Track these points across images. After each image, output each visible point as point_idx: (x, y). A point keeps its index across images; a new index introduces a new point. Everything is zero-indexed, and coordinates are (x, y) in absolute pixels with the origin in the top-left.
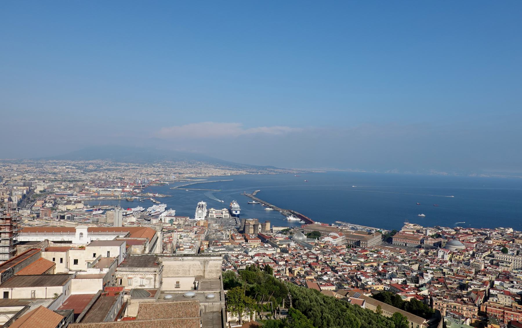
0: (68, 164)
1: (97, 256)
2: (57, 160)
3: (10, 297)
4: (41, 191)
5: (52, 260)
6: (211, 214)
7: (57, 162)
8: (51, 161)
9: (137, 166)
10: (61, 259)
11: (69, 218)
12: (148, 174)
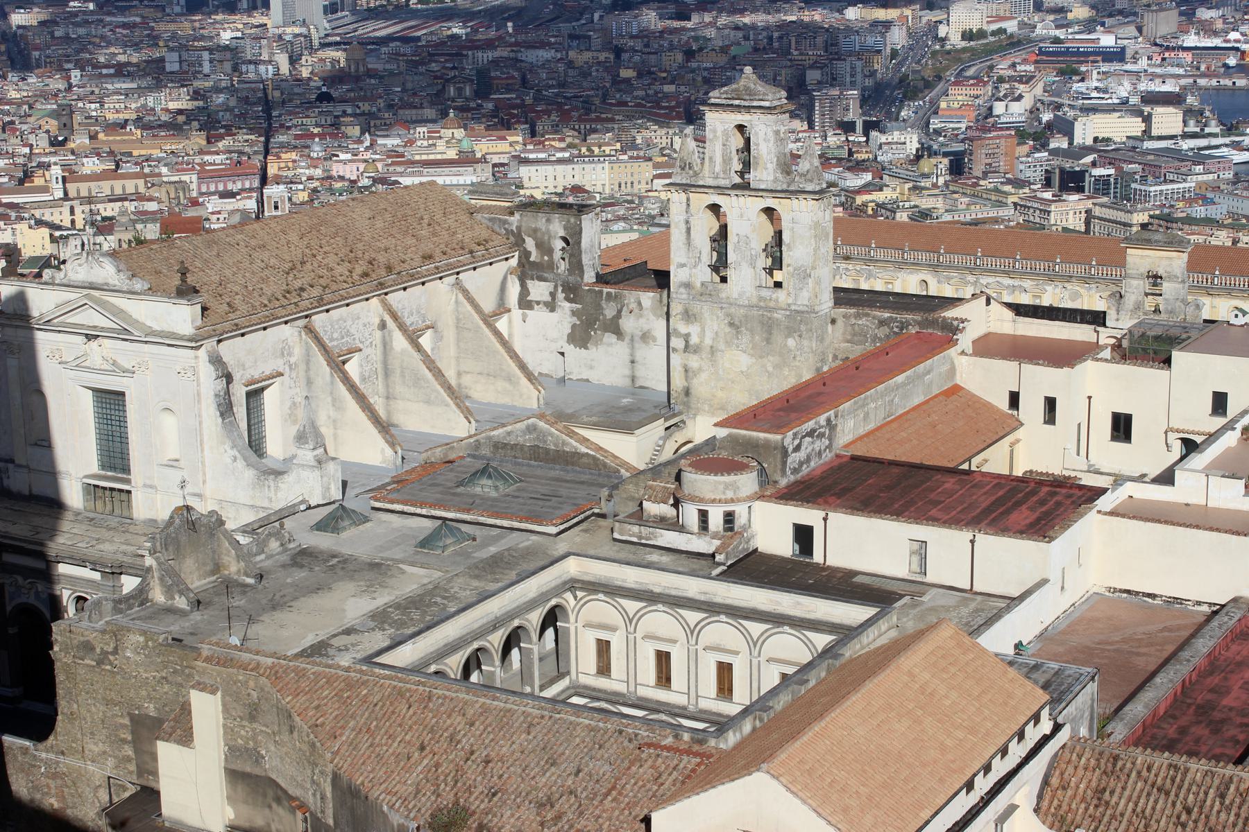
3: (818, 557)
4: (968, 35)
5: (1003, 404)
10: (1051, 404)
11: (1103, 186)
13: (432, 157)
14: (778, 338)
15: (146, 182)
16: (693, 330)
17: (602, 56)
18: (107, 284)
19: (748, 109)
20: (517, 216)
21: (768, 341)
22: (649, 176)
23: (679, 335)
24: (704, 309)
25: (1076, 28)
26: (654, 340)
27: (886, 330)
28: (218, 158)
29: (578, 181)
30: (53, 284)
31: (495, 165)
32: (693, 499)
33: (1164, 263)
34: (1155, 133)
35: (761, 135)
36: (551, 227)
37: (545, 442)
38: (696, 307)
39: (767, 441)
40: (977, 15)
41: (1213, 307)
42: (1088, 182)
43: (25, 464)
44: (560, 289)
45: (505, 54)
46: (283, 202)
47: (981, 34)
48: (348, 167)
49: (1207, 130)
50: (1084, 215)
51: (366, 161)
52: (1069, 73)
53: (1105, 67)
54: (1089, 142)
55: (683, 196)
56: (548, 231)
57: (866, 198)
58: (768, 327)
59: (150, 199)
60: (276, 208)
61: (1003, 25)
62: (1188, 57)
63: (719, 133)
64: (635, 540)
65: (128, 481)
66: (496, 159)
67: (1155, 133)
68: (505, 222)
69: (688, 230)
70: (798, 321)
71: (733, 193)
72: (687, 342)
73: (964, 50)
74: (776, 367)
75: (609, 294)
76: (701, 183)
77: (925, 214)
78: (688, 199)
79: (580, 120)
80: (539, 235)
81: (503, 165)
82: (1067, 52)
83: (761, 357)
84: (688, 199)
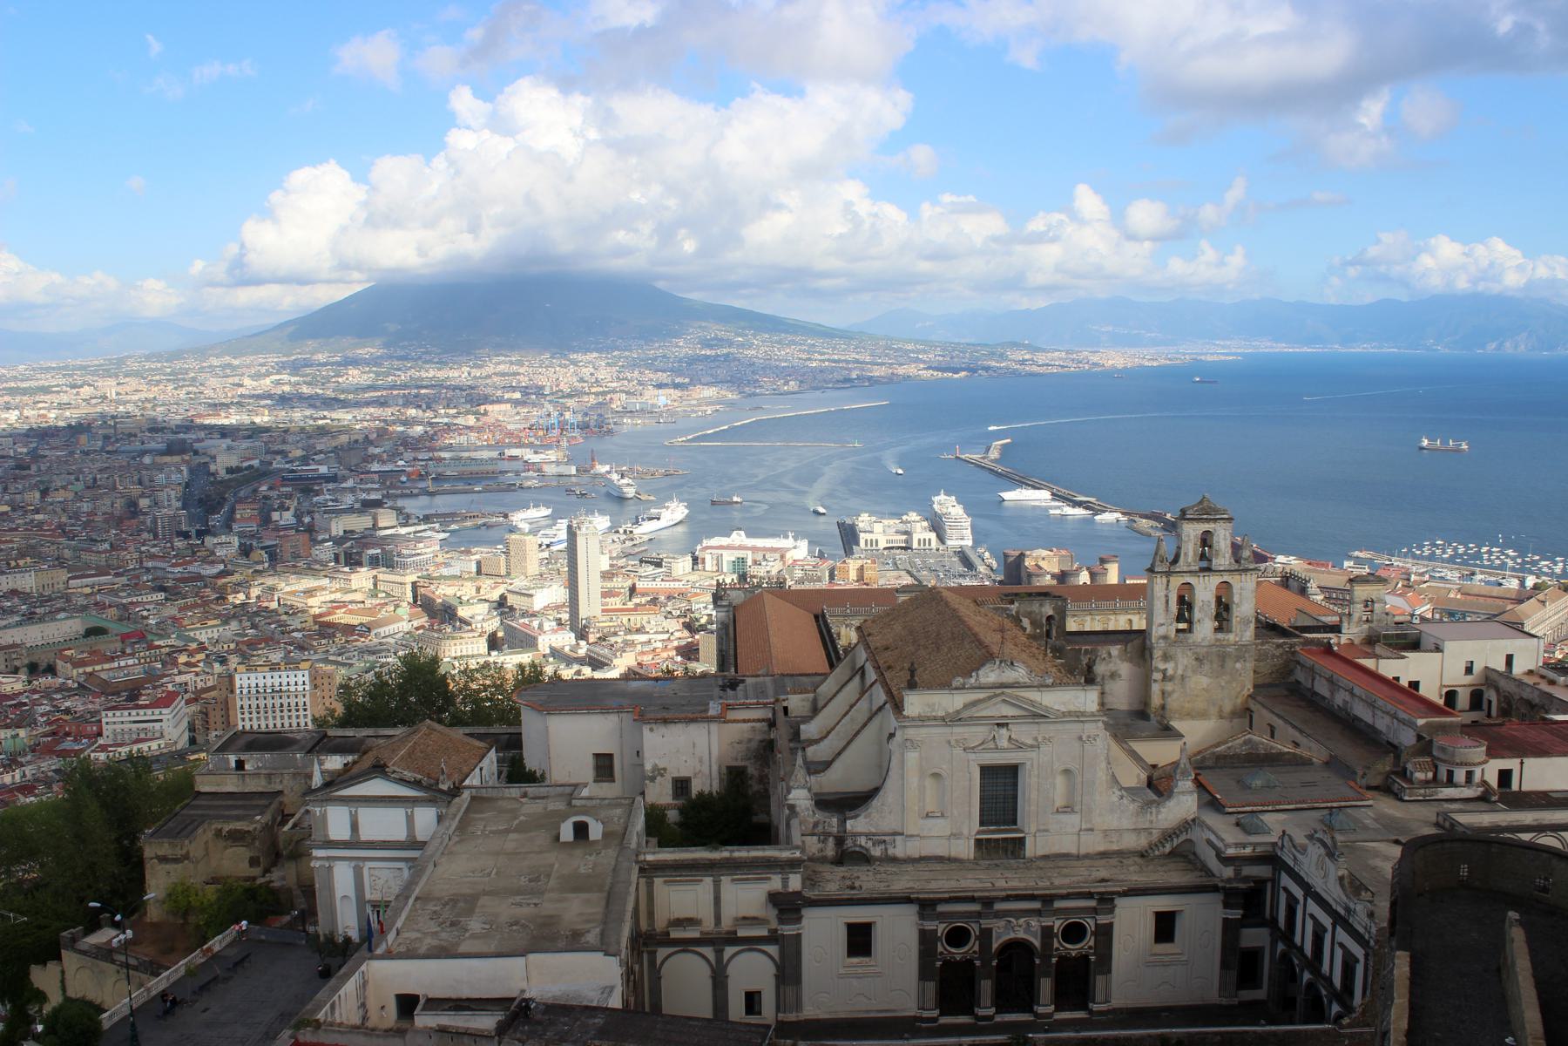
0: (273, 367)
1: (1477, 668)
2: (235, 358)
3: (1515, 787)
4: (230, 470)
6: (869, 536)
7: (236, 362)
8: (215, 362)
9: (512, 363)
12: (562, 391)
14: (1229, 664)
16: (1170, 667)
18: (1018, 683)
19: (1215, 520)
20: (1016, 604)
21: (1223, 666)
23: (1157, 670)
25: (297, 463)
26: (1120, 676)
29: (11, 586)
30: (963, 688)
32: (1461, 764)
33: (1375, 592)
34: (380, 525)
35: (1222, 536)
37: (1257, 749)
38: (1172, 651)
39: (1452, 722)
41: (1116, 621)
42: (365, 559)
43: (915, 833)
44: (1049, 651)
47: (238, 469)
50: (372, 580)
53: (331, 486)
54: (341, 533)
56: (1041, 613)
57: (224, 580)
58: (1223, 658)
62: (376, 477)
63: (1192, 537)
64: (1421, 798)
65: (1022, 832)
67: (380, 525)
70: (1241, 651)
71: (1201, 574)
72: (1164, 674)
73: (230, 480)
74: (1226, 683)
75: (1086, 650)
76: (1178, 570)
78: (1168, 581)
80: (1033, 615)
82: (301, 478)
84: (1168, 581)
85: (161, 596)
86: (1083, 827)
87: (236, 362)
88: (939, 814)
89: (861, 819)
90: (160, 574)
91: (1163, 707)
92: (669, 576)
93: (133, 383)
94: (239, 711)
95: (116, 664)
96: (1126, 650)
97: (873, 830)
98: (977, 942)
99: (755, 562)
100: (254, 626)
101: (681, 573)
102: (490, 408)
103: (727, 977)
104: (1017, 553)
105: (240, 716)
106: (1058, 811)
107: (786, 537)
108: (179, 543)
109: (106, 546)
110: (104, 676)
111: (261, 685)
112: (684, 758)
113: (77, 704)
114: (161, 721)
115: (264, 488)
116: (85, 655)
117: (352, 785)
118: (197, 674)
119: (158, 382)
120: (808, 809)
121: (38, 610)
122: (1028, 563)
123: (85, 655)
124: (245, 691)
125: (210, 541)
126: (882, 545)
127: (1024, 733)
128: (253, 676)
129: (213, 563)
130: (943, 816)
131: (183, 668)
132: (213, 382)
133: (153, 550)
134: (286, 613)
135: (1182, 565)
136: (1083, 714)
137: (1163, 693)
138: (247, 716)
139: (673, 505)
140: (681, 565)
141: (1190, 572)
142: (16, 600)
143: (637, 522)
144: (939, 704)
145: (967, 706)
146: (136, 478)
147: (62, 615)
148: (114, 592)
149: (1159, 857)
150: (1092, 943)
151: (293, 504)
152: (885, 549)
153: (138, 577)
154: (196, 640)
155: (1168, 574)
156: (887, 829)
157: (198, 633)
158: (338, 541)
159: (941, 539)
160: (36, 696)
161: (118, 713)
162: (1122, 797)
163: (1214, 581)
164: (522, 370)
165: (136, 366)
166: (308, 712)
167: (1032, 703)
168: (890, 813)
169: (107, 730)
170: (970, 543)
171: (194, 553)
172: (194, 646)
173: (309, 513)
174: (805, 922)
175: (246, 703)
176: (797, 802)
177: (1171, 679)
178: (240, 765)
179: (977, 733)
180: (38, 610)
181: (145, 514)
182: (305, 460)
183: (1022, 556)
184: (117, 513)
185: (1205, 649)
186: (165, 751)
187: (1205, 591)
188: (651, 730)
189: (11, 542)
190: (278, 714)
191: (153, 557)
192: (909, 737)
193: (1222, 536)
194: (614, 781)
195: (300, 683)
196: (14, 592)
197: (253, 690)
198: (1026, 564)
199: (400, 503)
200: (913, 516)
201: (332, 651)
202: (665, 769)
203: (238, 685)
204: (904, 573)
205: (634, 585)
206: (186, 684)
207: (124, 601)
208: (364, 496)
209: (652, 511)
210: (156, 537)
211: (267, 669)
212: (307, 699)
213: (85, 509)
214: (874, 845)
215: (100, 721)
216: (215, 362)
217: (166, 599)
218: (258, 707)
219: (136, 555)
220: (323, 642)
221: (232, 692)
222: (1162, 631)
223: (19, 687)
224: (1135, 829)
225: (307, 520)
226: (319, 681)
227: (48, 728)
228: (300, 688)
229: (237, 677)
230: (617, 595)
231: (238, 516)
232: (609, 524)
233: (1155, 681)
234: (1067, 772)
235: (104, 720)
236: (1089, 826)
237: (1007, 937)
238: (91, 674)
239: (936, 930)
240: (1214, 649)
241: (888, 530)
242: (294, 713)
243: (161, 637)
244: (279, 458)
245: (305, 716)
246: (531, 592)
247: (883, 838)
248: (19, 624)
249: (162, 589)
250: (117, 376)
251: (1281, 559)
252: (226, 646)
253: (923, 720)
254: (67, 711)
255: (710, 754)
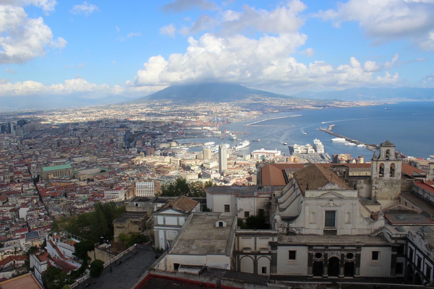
0: (146, 106)
2: (137, 104)
4: (135, 132)
6: (296, 150)
7: (137, 105)
8: (132, 105)
9: (205, 105)
12: (217, 112)
13: (55, 157)
14: (394, 185)
15: (4, 165)
16: (377, 186)
17: (77, 138)
18: (336, 189)
19: (390, 147)
20: (336, 168)
21: (392, 186)
22: (96, 158)
23: (374, 186)
24: (379, 182)
26: (363, 188)
27: (409, 182)
28: (16, 160)
29: (84, 160)
30: (321, 190)
31: (69, 158)
35: (392, 151)
36: (343, 170)
37: (402, 209)
38: (378, 181)
40: (136, 129)
41: (363, 173)
42: (168, 154)
43: (308, 228)
44: (344, 181)
45: (59, 139)
46: (35, 167)
47: (137, 132)
48: (41, 160)
49: (179, 145)
50: (170, 160)
51: (44, 159)
52: (154, 137)
53: (160, 136)
54: (162, 148)
55: (376, 162)
56: (342, 171)
57: (134, 159)
58: (392, 184)
59: (6, 168)
60: (34, 168)
61: (140, 130)
62: (171, 134)
63: (384, 151)
65: (336, 228)
66: (68, 157)
68: (333, 169)
69: (377, 168)
70: (397, 182)
71: (386, 161)
74: (393, 190)
77: (145, 161)
78: (377, 163)
79: (78, 149)
81: (70, 158)
82: (152, 134)
83: (391, 189)
84: (377, 163)
85: (118, 163)
86: (353, 228)
87: (137, 105)
88: (314, 223)
89: (293, 224)
90: (118, 157)
91: (375, 196)
92: (244, 160)
93: (112, 110)
94: (137, 192)
95: (108, 179)
96: (365, 181)
97: (297, 227)
98: (324, 257)
99: (267, 157)
100: (141, 171)
101: (248, 159)
102: (199, 116)
103: (257, 263)
104: (336, 155)
105: (137, 193)
106: (346, 223)
107: (275, 150)
108: (123, 150)
109: (106, 150)
110: (105, 182)
111: (142, 185)
112: (248, 207)
113: (98, 189)
114: (118, 193)
115: (143, 136)
116: (100, 177)
117: (164, 211)
118: (127, 182)
119: (118, 110)
120: (279, 221)
121: (90, 166)
122: (339, 157)
123: (100, 177)
124: (138, 187)
125: (130, 149)
126: (300, 152)
127: (337, 202)
128: (140, 183)
129: (131, 155)
130: (315, 223)
131: (123, 181)
132: (131, 110)
133: (116, 152)
134: (148, 168)
135: (381, 159)
136: (353, 198)
137: (375, 193)
138: (139, 193)
139: (246, 141)
140: (248, 157)
141: (383, 160)
142: (85, 163)
143: (236, 146)
144: (315, 194)
145: (322, 195)
146: (113, 134)
147: (95, 167)
148: (107, 162)
149: (374, 237)
150: (355, 259)
151: (150, 140)
152: (301, 153)
153: (113, 158)
154: (126, 174)
155: (377, 161)
156: (300, 227)
157: (127, 172)
158: (162, 150)
159: (316, 151)
160: (89, 187)
161: (108, 191)
162: (364, 220)
163: (390, 163)
164: (207, 107)
165: (113, 107)
166: (153, 192)
167: (339, 194)
168: (301, 222)
169: (105, 195)
170: (323, 152)
171: (126, 152)
172: (126, 175)
173: (155, 143)
174: (278, 250)
175: (138, 190)
176: (277, 219)
177: (378, 189)
178: (137, 205)
179: (325, 202)
180: (90, 166)
181: (115, 143)
182: (153, 130)
183: (337, 156)
184: (108, 142)
185: (387, 181)
186: (119, 201)
187: (387, 166)
188: (239, 199)
189: (84, 149)
190: (146, 192)
191: (117, 153)
192: (306, 202)
193: (392, 151)
194: (230, 212)
195: (152, 185)
196: (84, 161)
197: (140, 187)
198: (338, 158)
199: (177, 140)
200: (308, 145)
201: (159, 177)
202: (243, 209)
203: (136, 185)
204: (306, 160)
205: (236, 162)
206: (124, 185)
207: (110, 164)
208: (168, 139)
209: (241, 143)
210: (117, 148)
211: (144, 181)
212: (153, 189)
213: (101, 141)
214: (297, 230)
215: (104, 193)
216: (132, 105)
217: (120, 164)
218: (141, 191)
219: (113, 153)
220: (157, 175)
221: (135, 187)
222: (375, 176)
223: (85, 184)
224: (367, 229)
225: (154, 144)
226: (156, 185)
227: (92, 194)
228: (152, 186)
229: (136, 183)
230: (231, 164)
231: (137, 143)
232: (229, 146)
233: (373, 189)
234: (348, 213)
235: (105, 193)
236: (354, 228)
237: (332, 256)
238: (102, 182)
239: (313, 253)
240: (390, 181)
241: (302, 149)
242: (150, 193)
243: (118, 173)
244: (147, 129)
245: (153, 193)
246: (209, 163)
247: (299, 229)
248: (85, 169)
249: (119, 161)
250: (109, 109)
251: (409, 157)
252: (134, 176)
253: (310, 198)
254: (96, 190)
255: (254, 205)
